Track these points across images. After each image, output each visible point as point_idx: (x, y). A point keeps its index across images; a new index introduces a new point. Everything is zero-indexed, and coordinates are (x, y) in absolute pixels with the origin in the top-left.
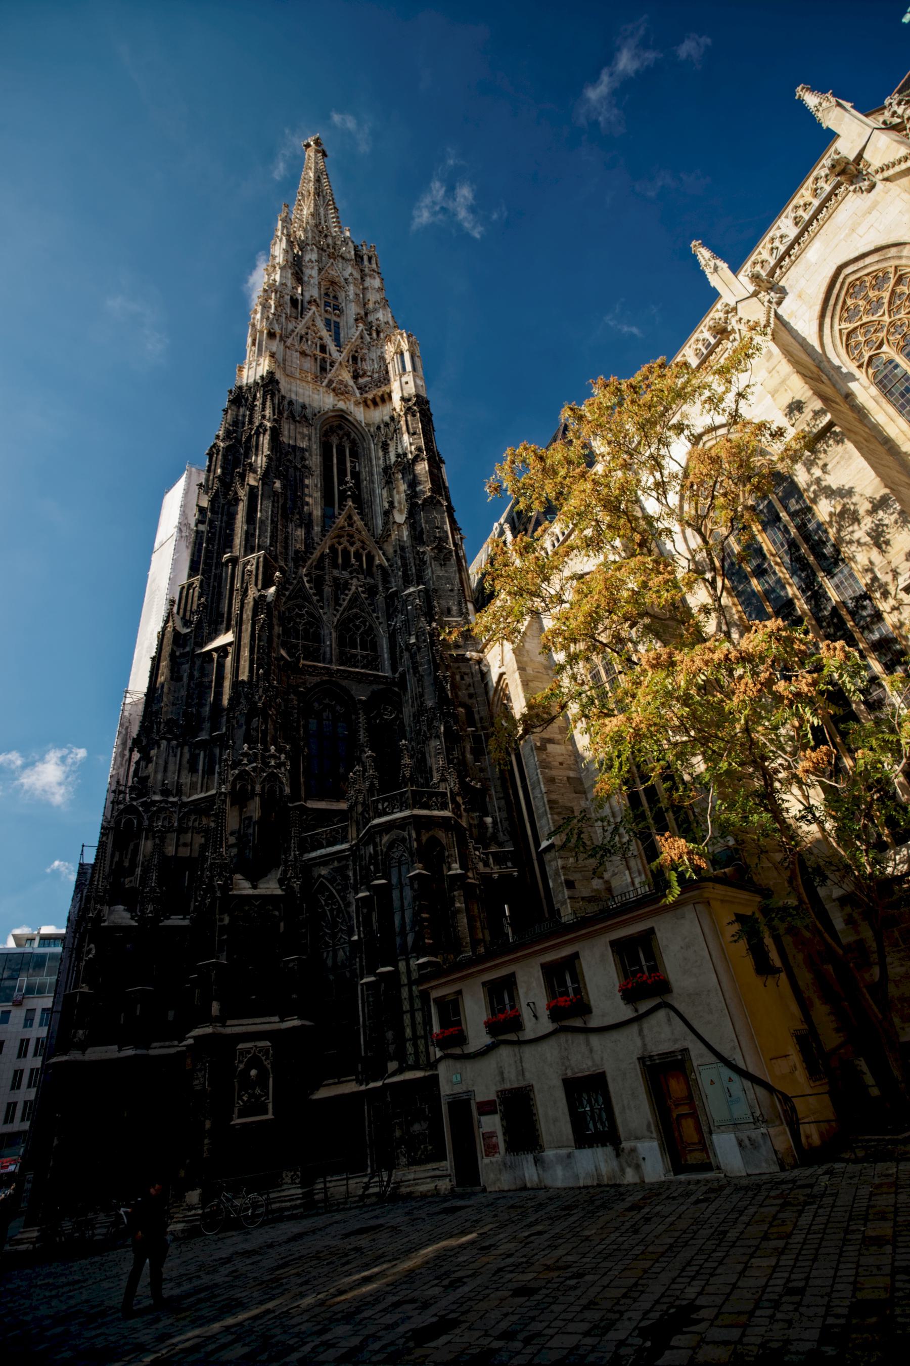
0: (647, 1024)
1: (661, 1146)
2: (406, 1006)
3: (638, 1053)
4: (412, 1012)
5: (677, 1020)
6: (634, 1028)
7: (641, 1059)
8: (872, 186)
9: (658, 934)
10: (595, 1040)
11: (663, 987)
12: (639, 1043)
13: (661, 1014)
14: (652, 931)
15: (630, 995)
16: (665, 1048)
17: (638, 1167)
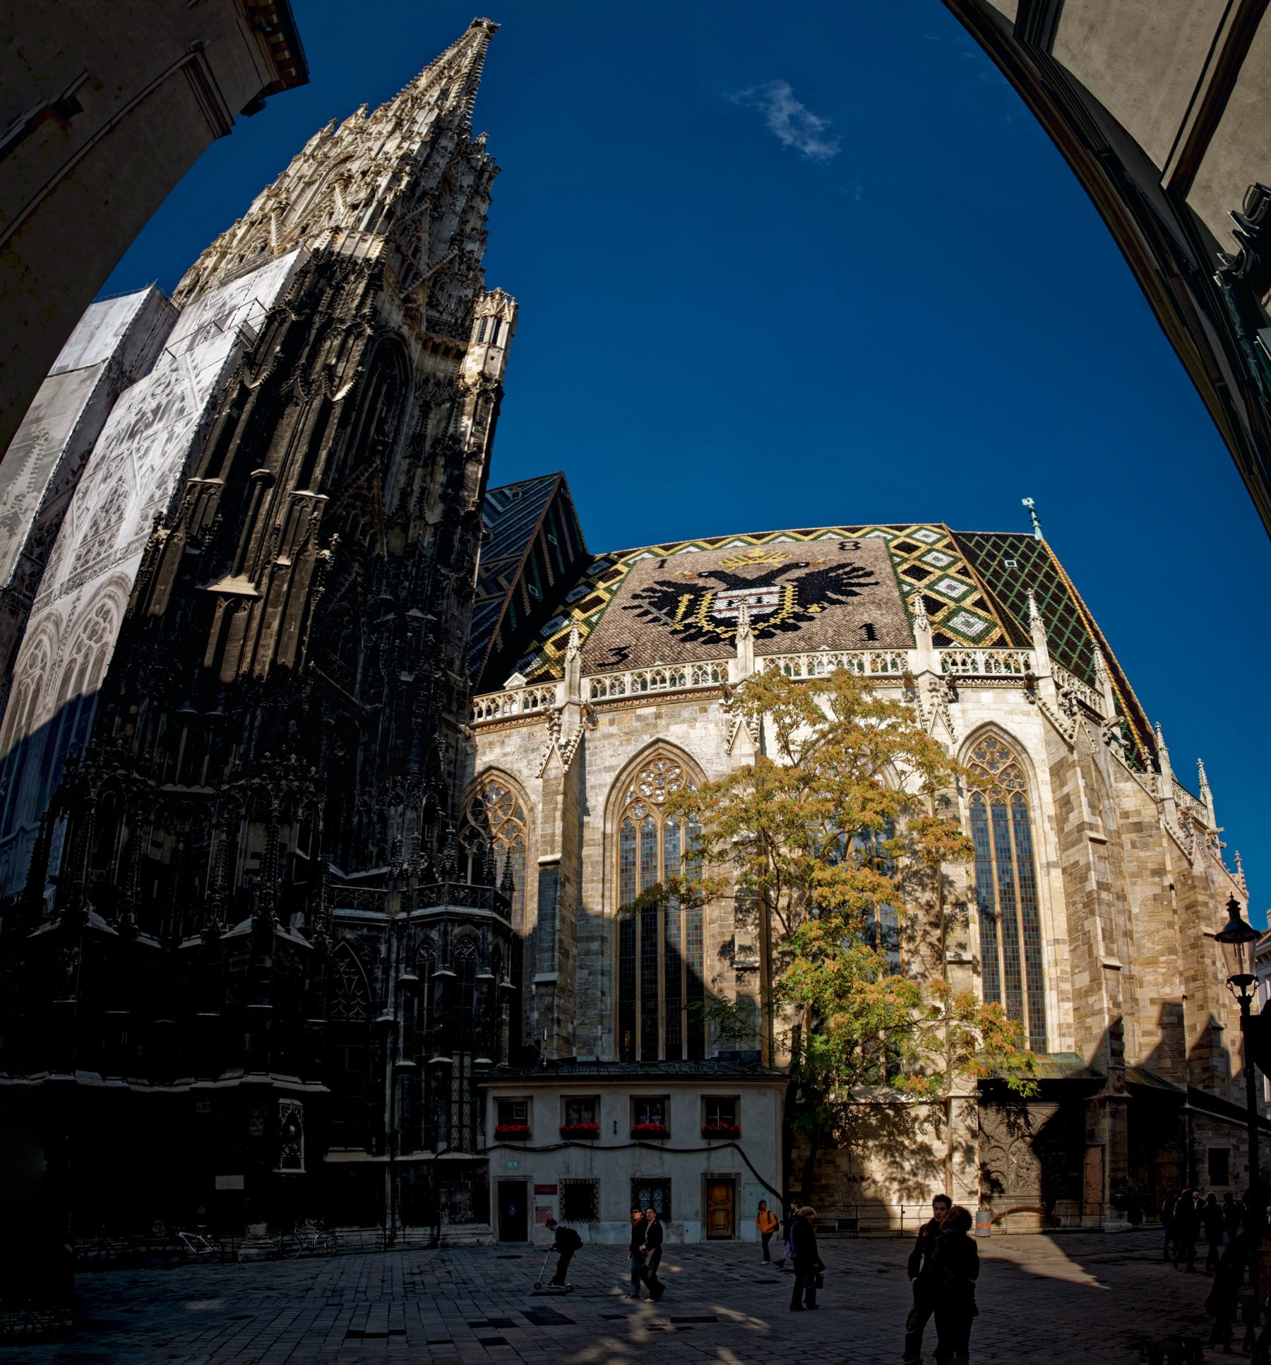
0: (714, 1154)
1: (703, 1225)
2: (455, 1097)
3: (703, 1170)
4: (461, 1103)
5: (739, 1155)
6: (704, 1155)
7: (704, 1175)
8: (1032, 703)
9: (742, 1101)
10: (667, 1157)
11: (736, 1134)
12: (705, 1164)
13: (729, 1150)
14: (738, 1097)
15: (707, 1134)
16: (723, 1170)
17: (681, 1235)
